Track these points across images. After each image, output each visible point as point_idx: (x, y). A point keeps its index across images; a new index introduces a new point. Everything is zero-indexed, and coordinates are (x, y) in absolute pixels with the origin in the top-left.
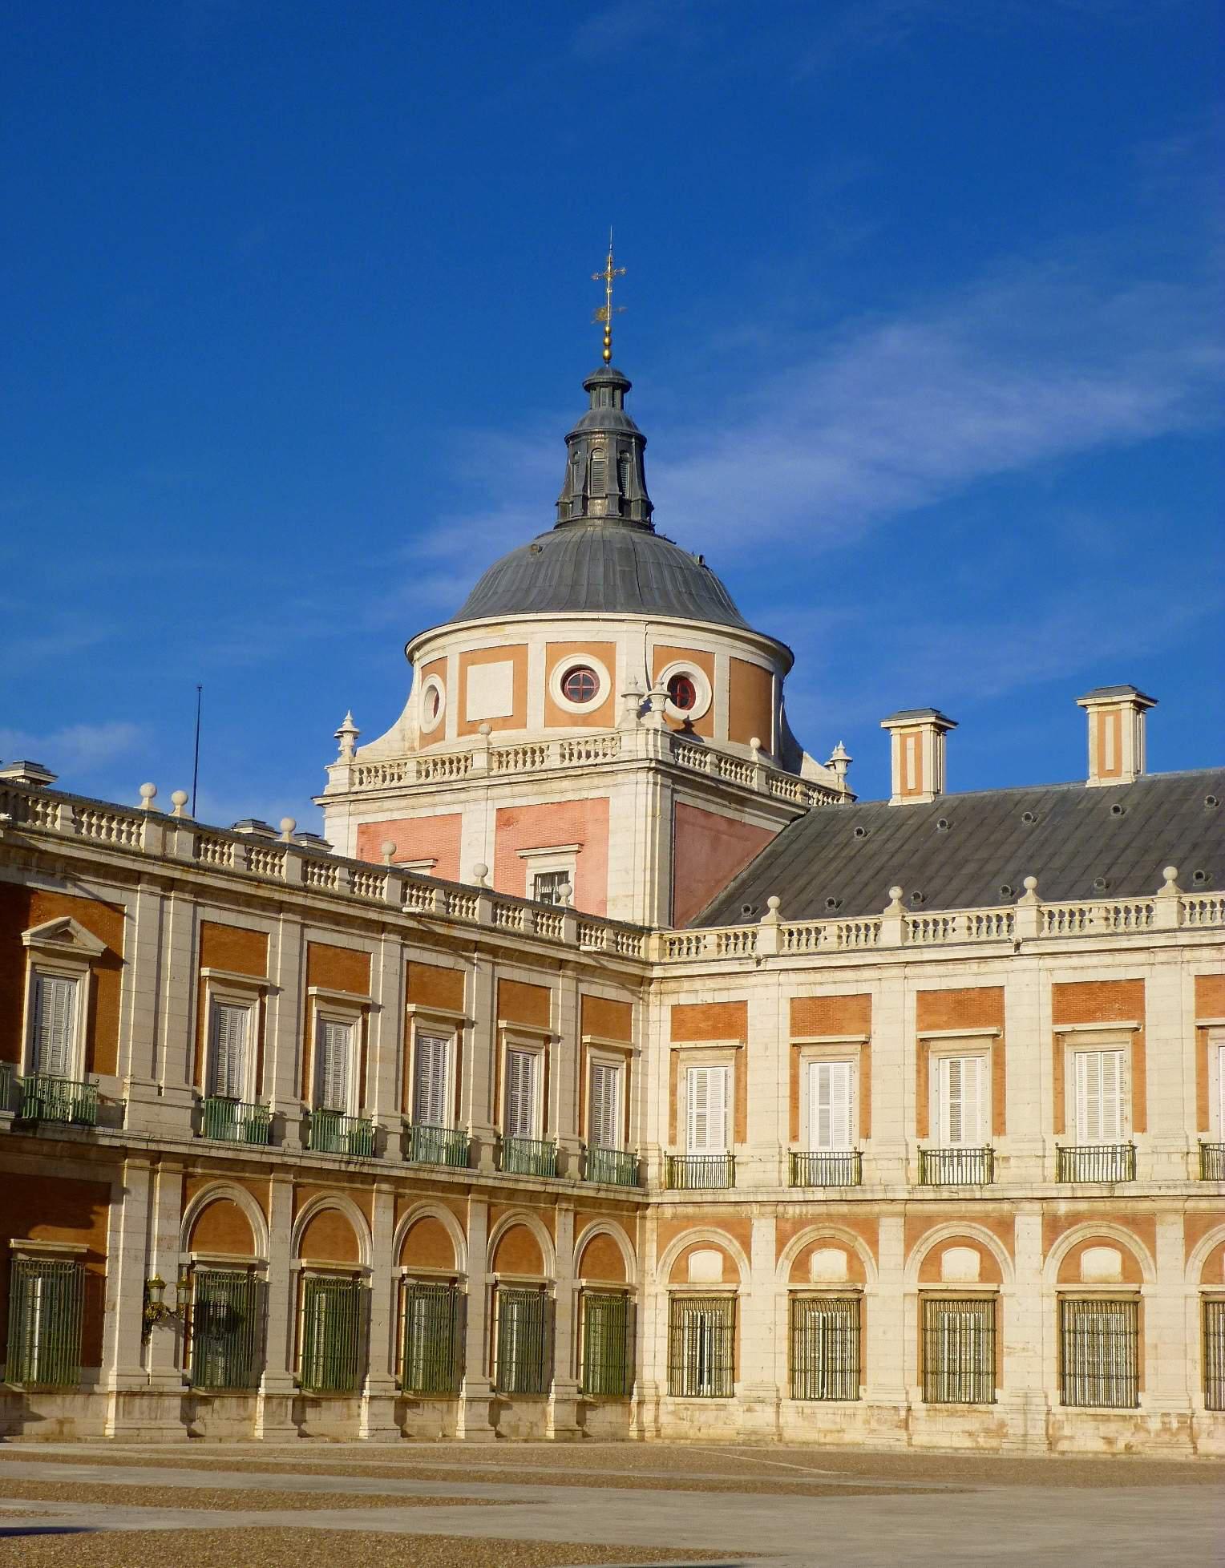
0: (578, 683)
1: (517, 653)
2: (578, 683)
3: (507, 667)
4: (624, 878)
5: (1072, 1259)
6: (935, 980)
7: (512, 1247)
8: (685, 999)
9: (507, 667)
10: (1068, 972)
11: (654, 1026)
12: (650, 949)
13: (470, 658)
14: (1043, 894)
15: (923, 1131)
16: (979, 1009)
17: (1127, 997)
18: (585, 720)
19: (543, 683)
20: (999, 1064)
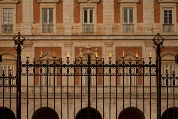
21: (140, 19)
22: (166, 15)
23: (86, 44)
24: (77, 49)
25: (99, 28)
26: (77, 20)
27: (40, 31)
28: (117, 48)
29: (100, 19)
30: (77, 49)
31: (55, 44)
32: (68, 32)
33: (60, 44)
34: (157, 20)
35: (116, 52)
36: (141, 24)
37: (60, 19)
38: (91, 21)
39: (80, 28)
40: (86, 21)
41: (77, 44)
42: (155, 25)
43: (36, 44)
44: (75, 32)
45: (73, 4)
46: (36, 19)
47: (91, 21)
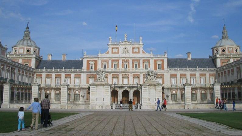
0: (28, 51)
1: (24, 48)
2: (28, 51)
3: (23, 49)
4: (33, 65)
5: (75, 92)
6: (56, 74)
7: (26, 91)
8: (37, 74)
9: (23, 49)
10: (66, 74)
11: (35, 75)
12: (35, 70)
13: (19, 48)
14: (64, 68)
15: (55, 83)
16: (60, 76)
17: (70, 75)
18: (28, 53)
19: (25, 50)
20: (61, 79)
21: (139, 67)
22: (146, 66)
23: (125, 73)
24: (123, 75)
25: (128, 69)
26: (123, 67)
27: (113, 70)
28: (133, 74)
29: (129, 67)
30: (123, 75)
31: (117, 73)
32: (120, 70)
33: (118, 73)
34: (143, 67)
35: (133, 75)
36: (139, 68)
37: (118, 67)
38: (126, 67)
39: (124, 69)
40: (125, 67)
41: (123, 73)
42: (143, 68)
43: (112, 74)
44: (122, 70)
45: (122, 63)
46: (112, 67)
47: (126, 67)
